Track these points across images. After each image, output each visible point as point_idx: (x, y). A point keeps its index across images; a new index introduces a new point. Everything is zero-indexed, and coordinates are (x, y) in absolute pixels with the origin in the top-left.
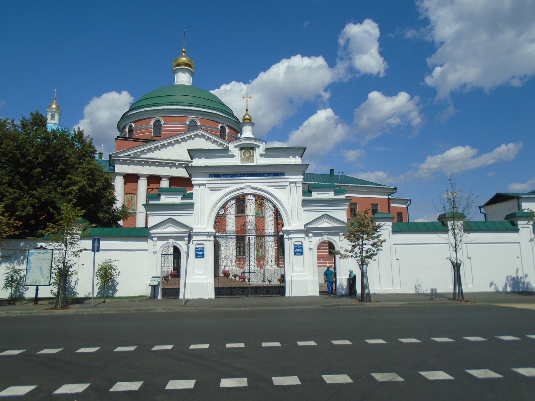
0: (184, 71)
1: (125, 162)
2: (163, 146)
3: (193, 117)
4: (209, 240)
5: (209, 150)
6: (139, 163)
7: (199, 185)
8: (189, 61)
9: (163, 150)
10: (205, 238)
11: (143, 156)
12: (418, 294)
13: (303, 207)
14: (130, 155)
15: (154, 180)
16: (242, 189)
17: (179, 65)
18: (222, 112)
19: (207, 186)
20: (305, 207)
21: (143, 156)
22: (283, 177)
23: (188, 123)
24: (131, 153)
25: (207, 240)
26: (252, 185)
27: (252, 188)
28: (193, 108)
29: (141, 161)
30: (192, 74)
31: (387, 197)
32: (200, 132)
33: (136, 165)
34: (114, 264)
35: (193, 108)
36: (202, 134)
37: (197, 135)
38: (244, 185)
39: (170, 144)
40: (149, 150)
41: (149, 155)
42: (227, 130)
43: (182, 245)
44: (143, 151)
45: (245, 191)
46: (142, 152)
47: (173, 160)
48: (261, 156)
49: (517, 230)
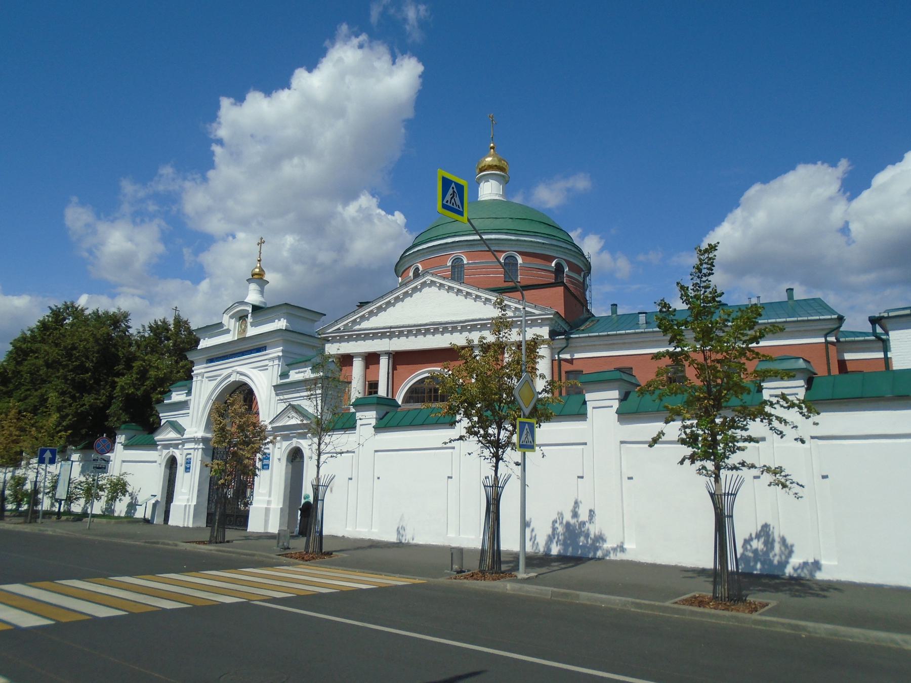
0: (486, 178)
1: (334, 340)
2: (380, 309)
3: (457, 253)
4: (198, 449)
5: (207, 326)
6: (350, 339)
7: (202, 375)
8: (500, 160)
9: (382, 315)
10: (192, 445)
11: (357, 327)
12: (399, 545)
13: (277, 395)
14: (339, 329)
15: (371, 359)
16: (229, 376)
17: (481, 170)
18: (506, 234)
19: (206, 375)
20: (282, 394)
21: (357, 327)
22: (264, 353)
23: (449, 264)
24: (340, 325)
25: (195, 449)
26: (239, 369)
27: (238, 373)
28: (457, 239)
29: (537, 319)
30: (504, 181)
31: (822, 340)
32: (429, 278)
33: (348, 341)
34: (127, 479)
35: (457, 239)
36: (432, 281)
37: (424, 285)
38: (230, 371)
39: (389, 304)
40: (363, 318)
41: (365, 325)
42: (520, 260)
43: (177, 453)
44: (355, 320)
45: (232, 379)
46: (354, 322)
47: (391, 328)
48: (253, 325)
49: (581, 415)
